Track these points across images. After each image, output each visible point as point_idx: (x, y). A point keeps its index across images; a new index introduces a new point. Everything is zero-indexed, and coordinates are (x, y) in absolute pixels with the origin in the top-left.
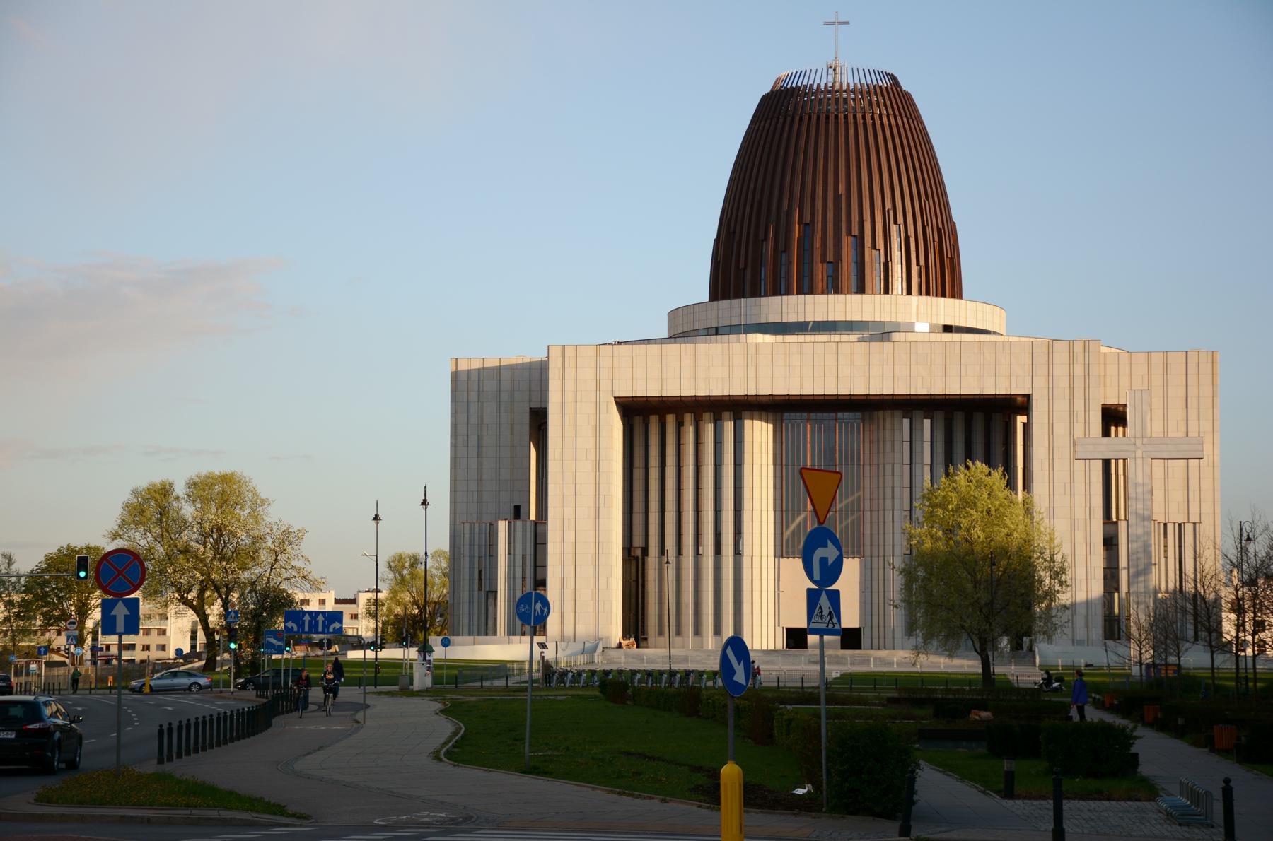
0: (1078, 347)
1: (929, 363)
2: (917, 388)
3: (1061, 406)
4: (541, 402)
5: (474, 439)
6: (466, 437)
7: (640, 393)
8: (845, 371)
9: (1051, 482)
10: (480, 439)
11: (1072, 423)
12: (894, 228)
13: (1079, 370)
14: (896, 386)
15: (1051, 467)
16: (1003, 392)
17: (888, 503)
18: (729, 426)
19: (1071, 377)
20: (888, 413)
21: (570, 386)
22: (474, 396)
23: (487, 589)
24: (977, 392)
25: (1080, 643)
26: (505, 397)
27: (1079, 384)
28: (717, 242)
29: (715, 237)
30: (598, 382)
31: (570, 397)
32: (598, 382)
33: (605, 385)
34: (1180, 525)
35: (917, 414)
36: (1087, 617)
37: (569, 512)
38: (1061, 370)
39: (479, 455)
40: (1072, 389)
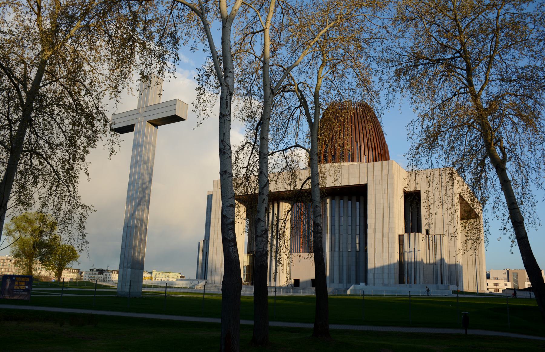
3: (379, 187)
9: (375, 218)
11: (383, 194)
12: (355, 143)
13: (385, 172)
16: (357, 184)
18: (276, 205)
19: (382, 175)
24: (347, 184)
25: (386, 285)
27: (385, 178)
34: (434, 236)
35: (346, 198)
36: (388, 274)
40: (382, 180)
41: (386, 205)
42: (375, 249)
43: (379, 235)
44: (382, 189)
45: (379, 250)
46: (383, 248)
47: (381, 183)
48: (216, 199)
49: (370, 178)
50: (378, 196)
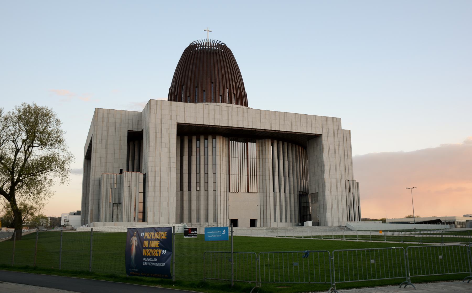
0: (335, 120)
1: (291, 120)
2: (287, 129)
3: (331, 139)
4: (132, 128)
5: (104, 141)
6: (101, 140)
7: (188, 122)
8: (263, 121)
10: (107, 141)
13: (336, 127)
14: (280, 128)
15: (329, 159)
16: (314, 133)
17: (267, 172)
19: (334, 129)
20: (266, 140)
21: (159, 117)
22: (105, 124)
23: (113, 203)
26: (118, 125)
27: (336, 132)
28: (171, 89)
29: (170, 87)
30: (171, 116)
31: (159, 121)
32: (171, 116)
33: (174, 117)
37: (158, 169)
38: (330, 127)
39: (106, 148)
40: (334, 133)
41: (337, 155)
42: (331, 192)
43: (333, 180)
44: (334, 141)
45: (334, 193)
46: (337, 191)
47: (333, 136)
48: (156, 123)
49: (325, 130)
50: (332, 147)
